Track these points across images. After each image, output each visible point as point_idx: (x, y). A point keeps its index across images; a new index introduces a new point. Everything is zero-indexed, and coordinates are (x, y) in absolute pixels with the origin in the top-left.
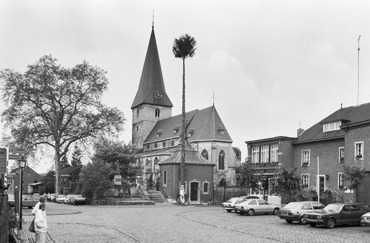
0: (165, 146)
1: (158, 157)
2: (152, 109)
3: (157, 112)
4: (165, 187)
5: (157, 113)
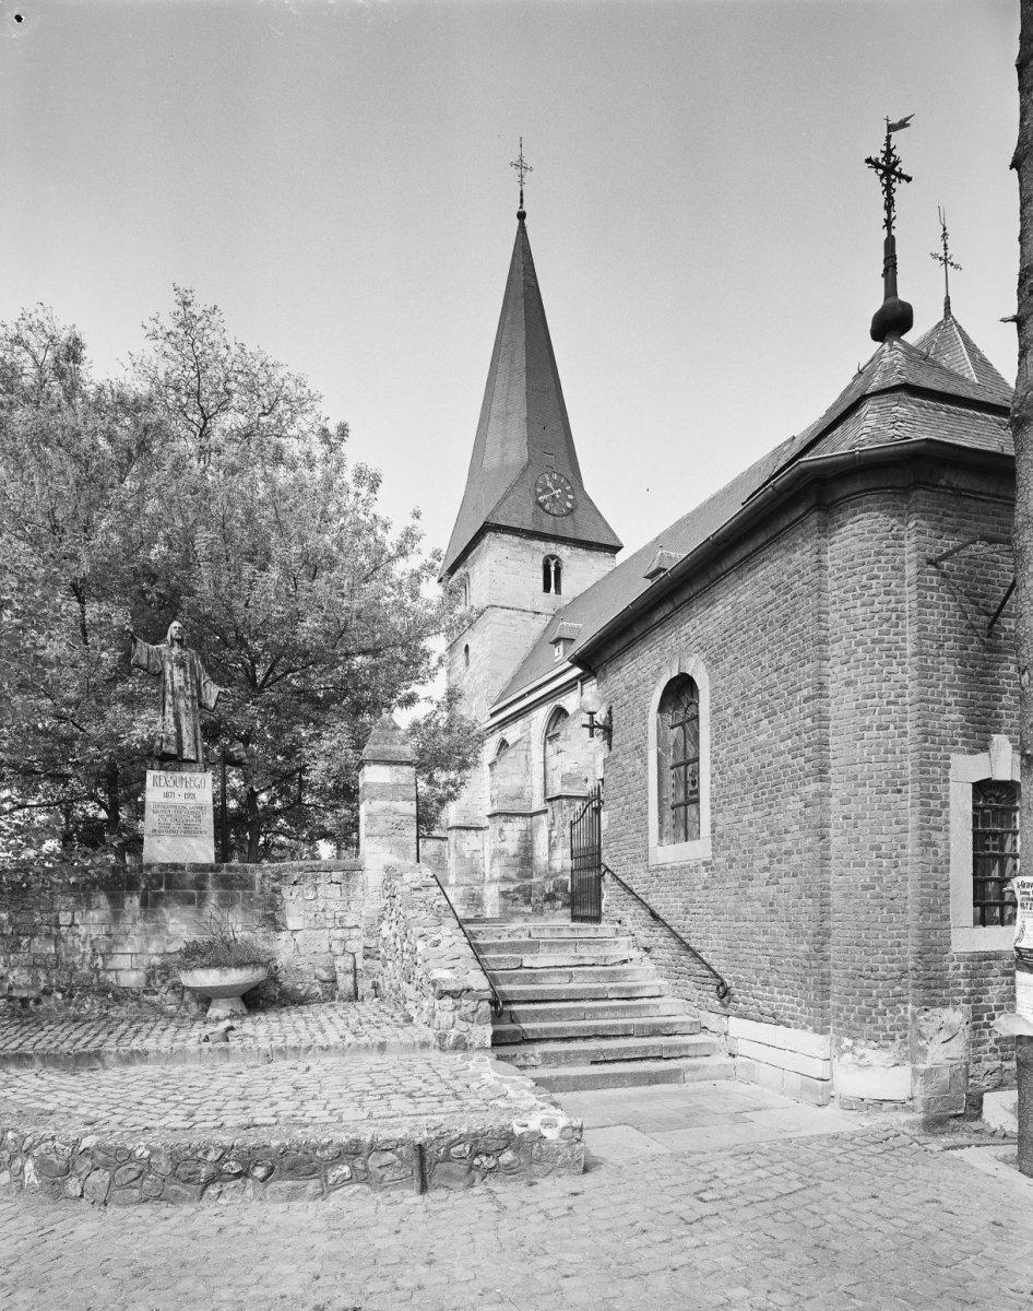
2: (526, 556)
3: (553, 568)
4: (679, 876)
5: (551, 576)
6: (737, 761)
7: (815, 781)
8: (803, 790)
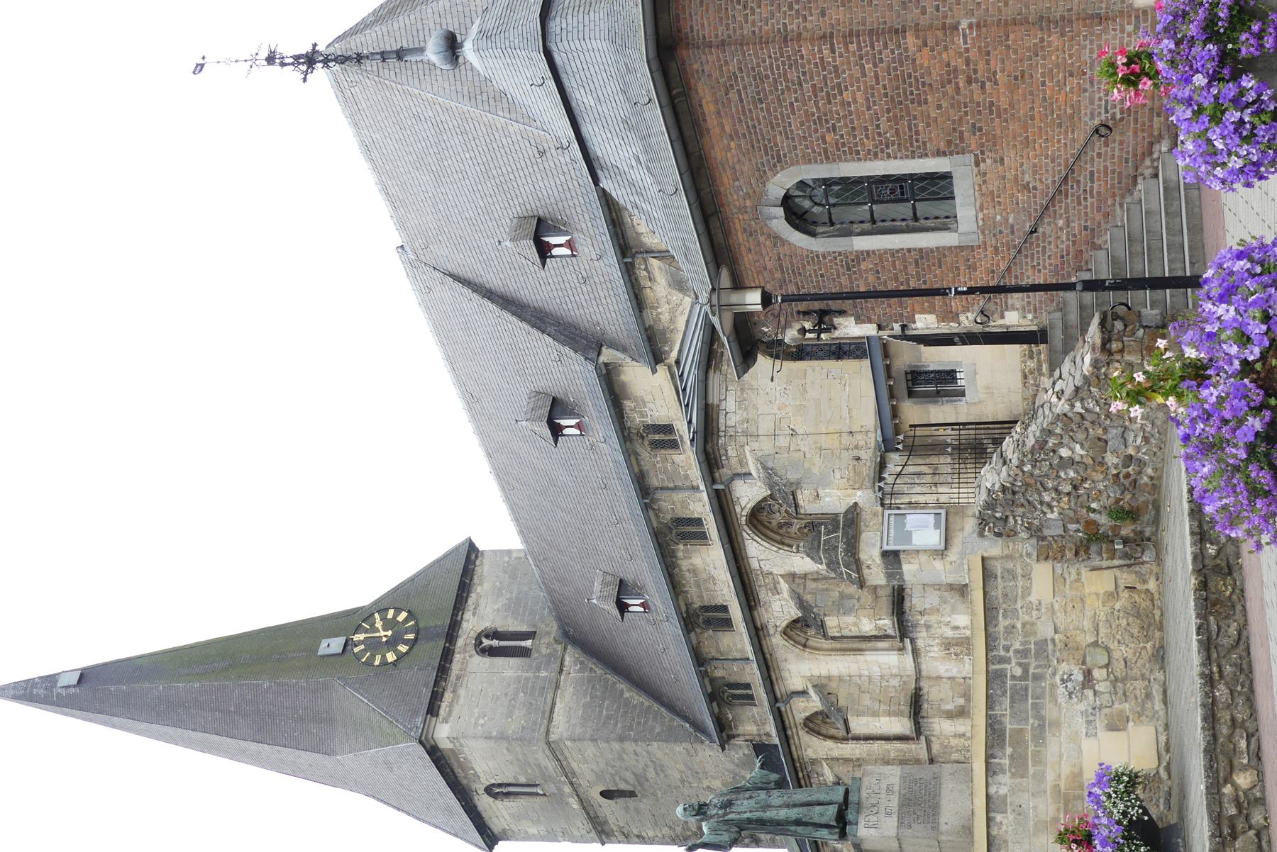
0: (698, 522)
1: (747, 494)
3: (495, 643)
4: (988, 198)
6: (878, 126)
7: (904, 38)
8: (912, 49)
